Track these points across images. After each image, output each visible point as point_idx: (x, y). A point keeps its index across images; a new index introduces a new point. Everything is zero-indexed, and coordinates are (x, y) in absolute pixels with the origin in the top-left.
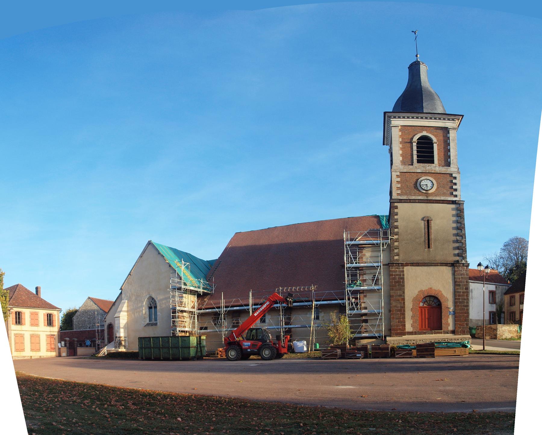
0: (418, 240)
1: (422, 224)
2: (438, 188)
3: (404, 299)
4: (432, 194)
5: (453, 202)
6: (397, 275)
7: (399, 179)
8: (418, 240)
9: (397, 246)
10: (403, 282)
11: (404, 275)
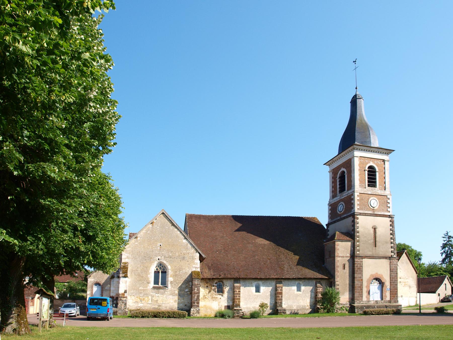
0: (369, 242)
1: (372, 231)
3: (362, 280)
4: (376, 210)
5: (389, 216)
6: (359, 264)
7: (358, 198)
8: (369, 242)
9: (359, 245)
10: (362, 268)
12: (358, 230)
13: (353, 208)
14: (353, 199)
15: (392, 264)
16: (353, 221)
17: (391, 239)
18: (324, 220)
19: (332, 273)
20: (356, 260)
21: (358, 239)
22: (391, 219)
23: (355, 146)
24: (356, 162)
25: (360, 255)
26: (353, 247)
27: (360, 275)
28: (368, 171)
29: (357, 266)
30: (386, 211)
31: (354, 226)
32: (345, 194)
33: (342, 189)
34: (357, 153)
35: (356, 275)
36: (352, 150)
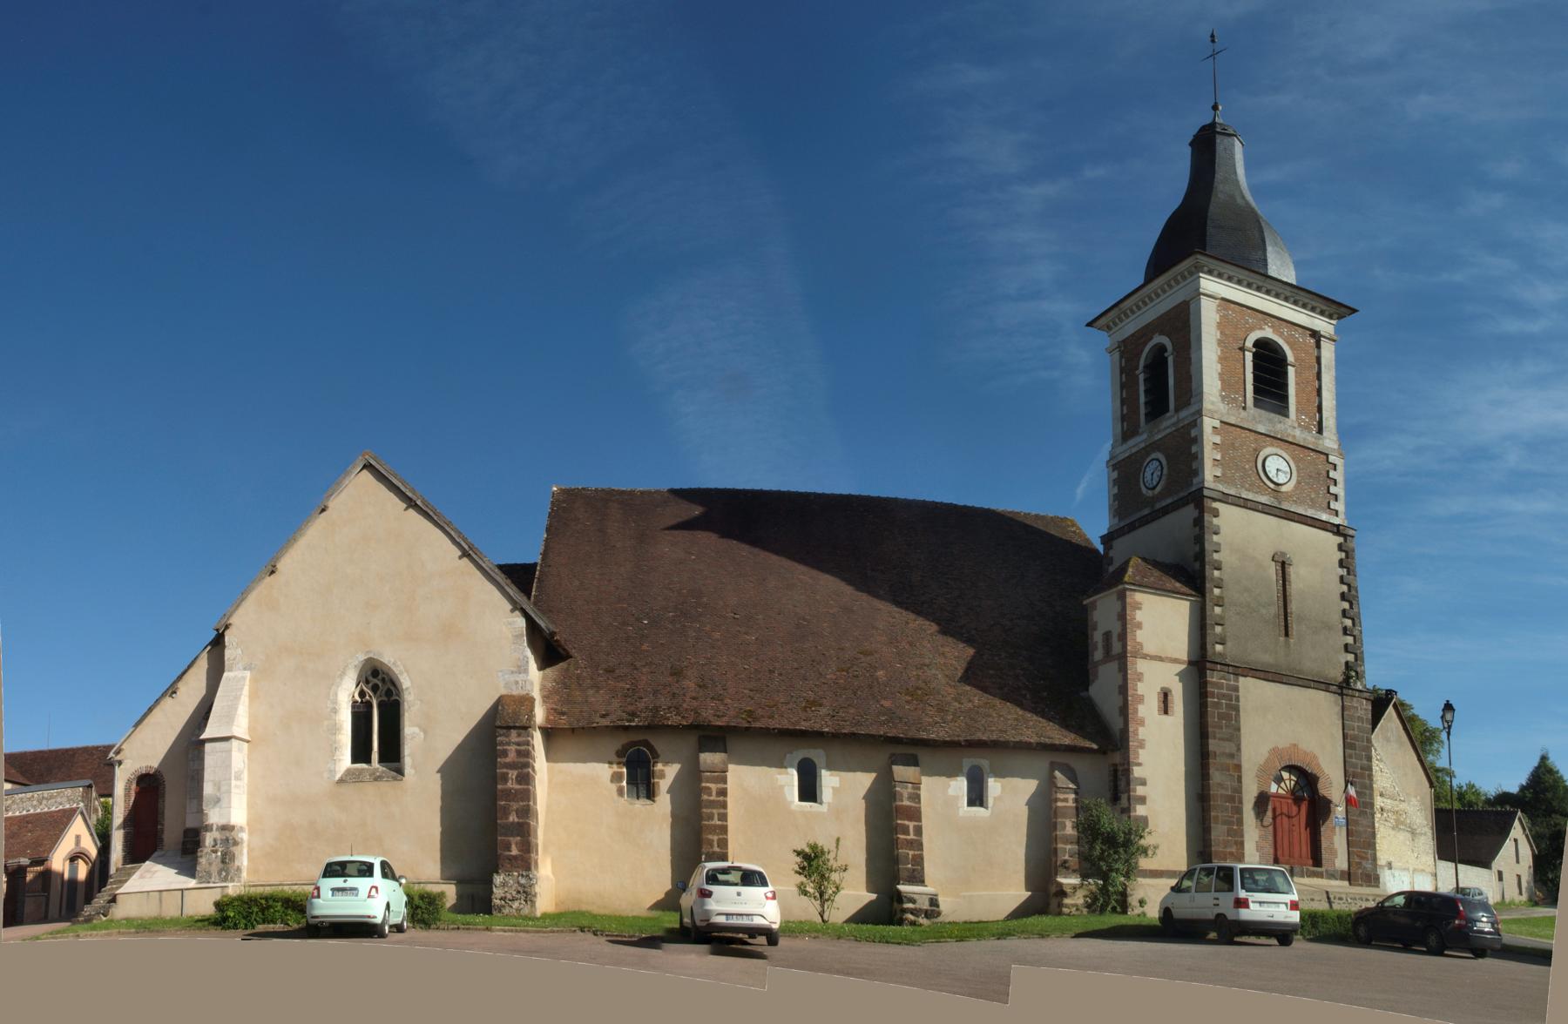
0: (1264, 611)
1: (1272, 570)
2: (1299, 482)
3: (1238, 767)
4: (1288, 496)
5: (1337, 530)
7: (1218, 439)
8: (1264, 611)
10: (1238, 715)
11: (1237, 699)
12: (1216, 556)
13: (1197, 472)
14: (1198, 440)
15: (1352, 718)
16: (1199, 522)
17: (1344, 613)
18: (1093, 525)
19: (1116, 723)
20: (1213, 677)
21: (1217, 591)
22: (1341, 540)
23: (1202, 259)
24: (1209, 315)
25: (1228, 661)
26: (1201, 627)
27: (1229, 747)
28: (1255, 355)
29: (1217, 705)
30: (1322, 509)
31: (1200, 540)
32: (1168, 424)
33: (1158, 407)
34: (1208, 284)
35: (1213, 745)
36: (1191, 274)
